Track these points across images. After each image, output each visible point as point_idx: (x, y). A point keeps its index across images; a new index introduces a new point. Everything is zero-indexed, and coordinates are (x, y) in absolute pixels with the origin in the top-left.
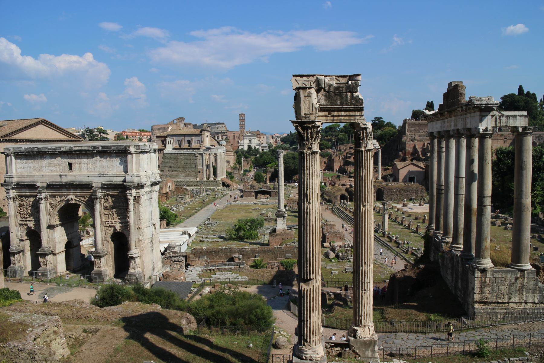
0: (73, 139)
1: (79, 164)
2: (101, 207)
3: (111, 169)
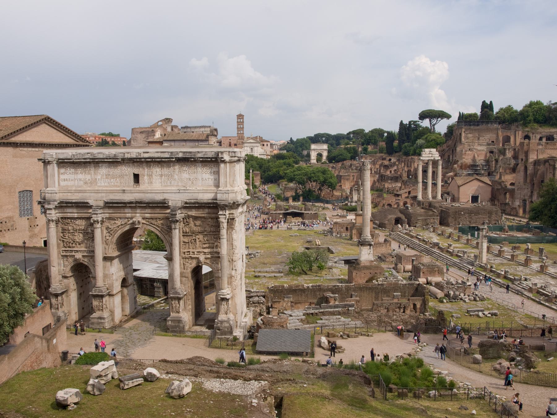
0: (81, 143)
1: (150, 176)
2: (179, 232)
3: (194, 182)
